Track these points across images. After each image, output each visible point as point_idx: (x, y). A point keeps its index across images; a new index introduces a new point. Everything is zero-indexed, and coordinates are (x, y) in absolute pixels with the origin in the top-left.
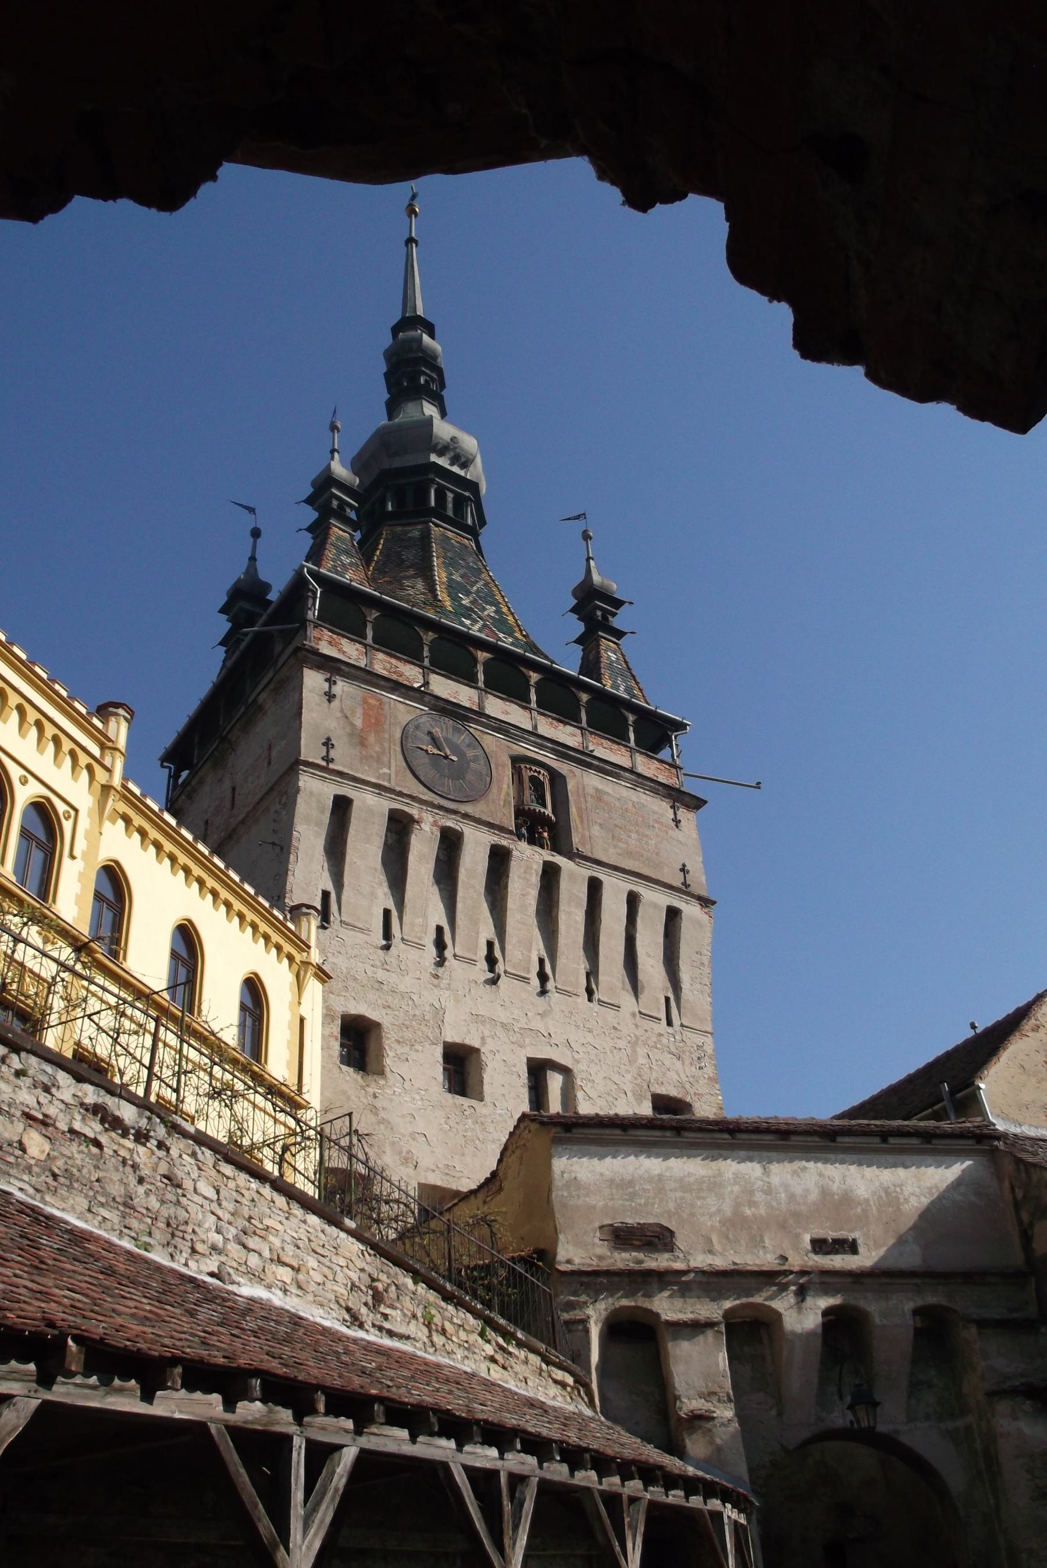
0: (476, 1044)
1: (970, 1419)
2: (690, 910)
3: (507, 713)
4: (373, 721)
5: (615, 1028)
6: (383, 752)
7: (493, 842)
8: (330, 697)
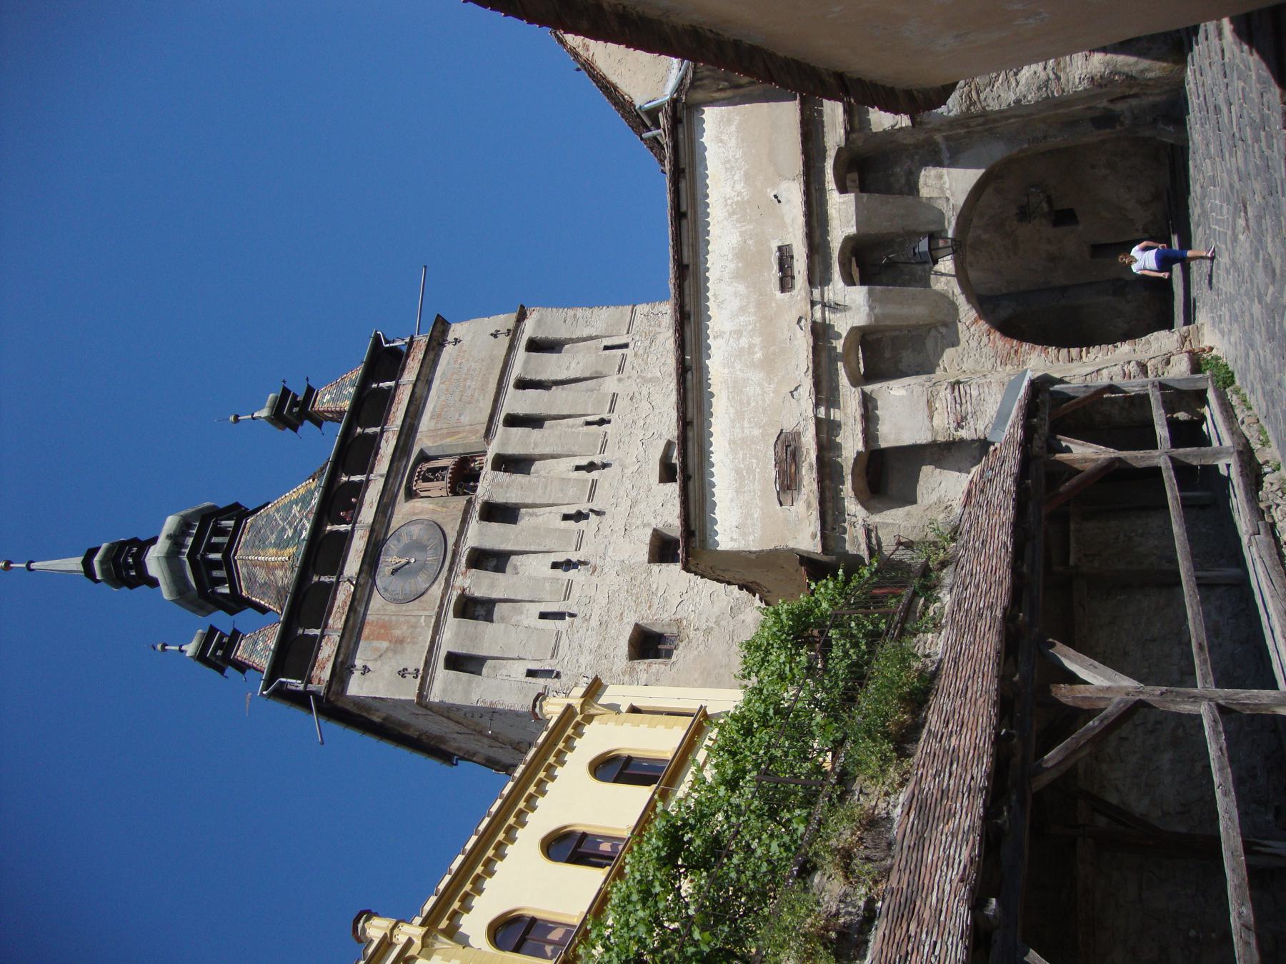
0: (649, 532)
1: (938, 137)
2: (529, 329)
3: (372, 503)
4: (382, 631)
5: (631, 399)
6: (408, 622)
7: (477, 518)
8: (366, 670)
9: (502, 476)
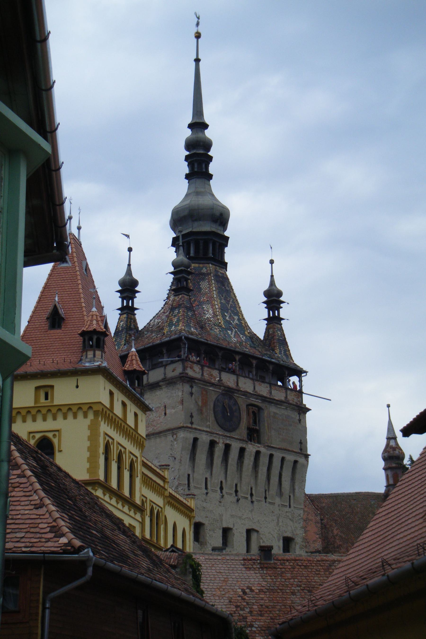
2: (301, 460)
4: (204, 401)
9: (254, 454)
